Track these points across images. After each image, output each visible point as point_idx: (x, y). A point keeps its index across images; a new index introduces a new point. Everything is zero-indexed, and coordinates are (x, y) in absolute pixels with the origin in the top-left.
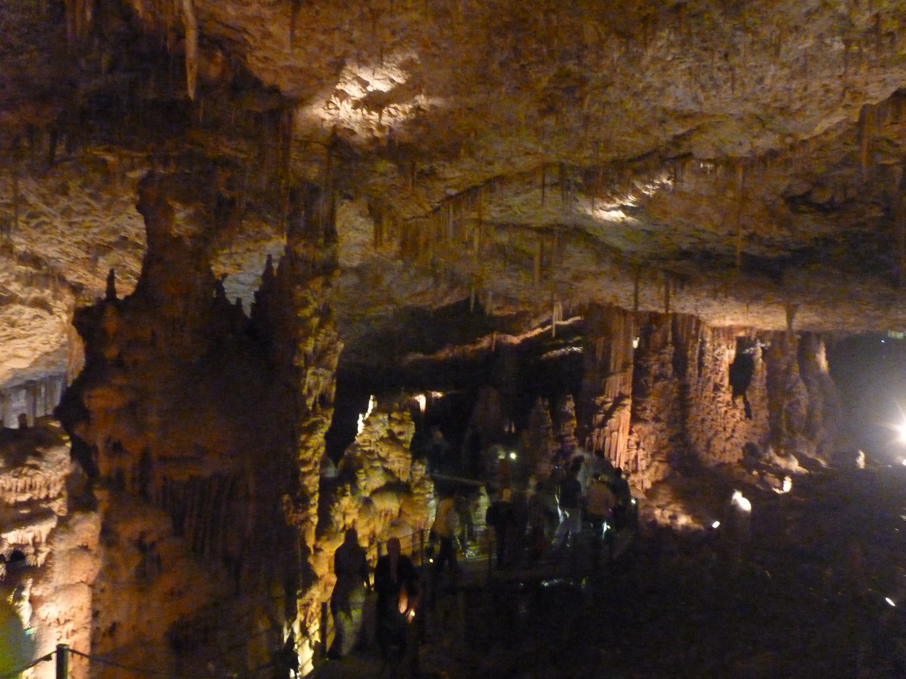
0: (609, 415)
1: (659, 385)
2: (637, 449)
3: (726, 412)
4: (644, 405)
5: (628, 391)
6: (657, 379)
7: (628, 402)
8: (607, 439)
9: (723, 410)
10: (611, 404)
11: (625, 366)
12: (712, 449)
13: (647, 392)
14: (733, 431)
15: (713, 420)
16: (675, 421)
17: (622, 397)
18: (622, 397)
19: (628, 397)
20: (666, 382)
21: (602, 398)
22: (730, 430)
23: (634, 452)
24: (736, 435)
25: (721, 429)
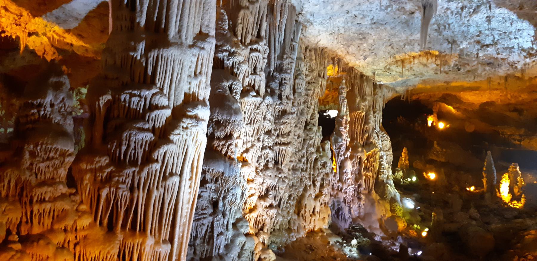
0: (163, 135)
1: (250, 100)
2: (214, 214)
3: (316, 160)
4: (228, 129)
5: (205, 93)
6: (245, 93)
7: (204, 113)
8: (155, 194)
9: (314, 156)
10: (168, 113)
11: (202, 36)
12: (302, 212)
13: (235, 106)
14: (322, 186)
15: (302, 170)
16: (266, 167)
17: (191, 101)
18: (191, 101)
19: (203, 103)
20: (259, 99)
21: (147, 93)
22: (318, 184)
23: (207, 221)
24: (325, 191)
25: (309, 183)
